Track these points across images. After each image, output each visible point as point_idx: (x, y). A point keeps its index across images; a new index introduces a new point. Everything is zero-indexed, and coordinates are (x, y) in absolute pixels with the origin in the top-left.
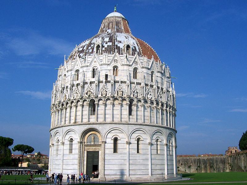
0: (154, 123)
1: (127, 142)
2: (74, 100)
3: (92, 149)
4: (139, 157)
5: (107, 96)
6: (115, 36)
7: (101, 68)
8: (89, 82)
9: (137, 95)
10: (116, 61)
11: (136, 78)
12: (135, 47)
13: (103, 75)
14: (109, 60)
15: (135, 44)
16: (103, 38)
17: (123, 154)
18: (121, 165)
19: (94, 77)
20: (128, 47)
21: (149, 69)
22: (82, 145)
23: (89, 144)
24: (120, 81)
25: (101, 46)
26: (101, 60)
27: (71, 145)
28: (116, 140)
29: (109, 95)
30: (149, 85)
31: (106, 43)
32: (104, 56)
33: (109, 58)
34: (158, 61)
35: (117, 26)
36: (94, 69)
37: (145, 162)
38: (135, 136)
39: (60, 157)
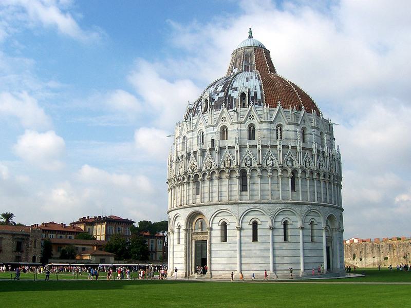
0: (278, 198)
3: (200, 238)
4: (255, 246)
8: (192, 152)
9: (251, 162)
10: (223, 119)
11: (254, 139)
12: (255, 93)
13: (208, 139)
14: (215, 119)
15: (258, 88)
17: (233, 243)
18: (231, 257)
20: (243, 95)
21: (271, 123)
22: (189, 234)
24: (227, 147)
25: (208, 99)
27: (179, 233)
30: (269, 145)
33: (215, 116)
34: (290, 107)
37: (265, 254)
38: (248, 218)
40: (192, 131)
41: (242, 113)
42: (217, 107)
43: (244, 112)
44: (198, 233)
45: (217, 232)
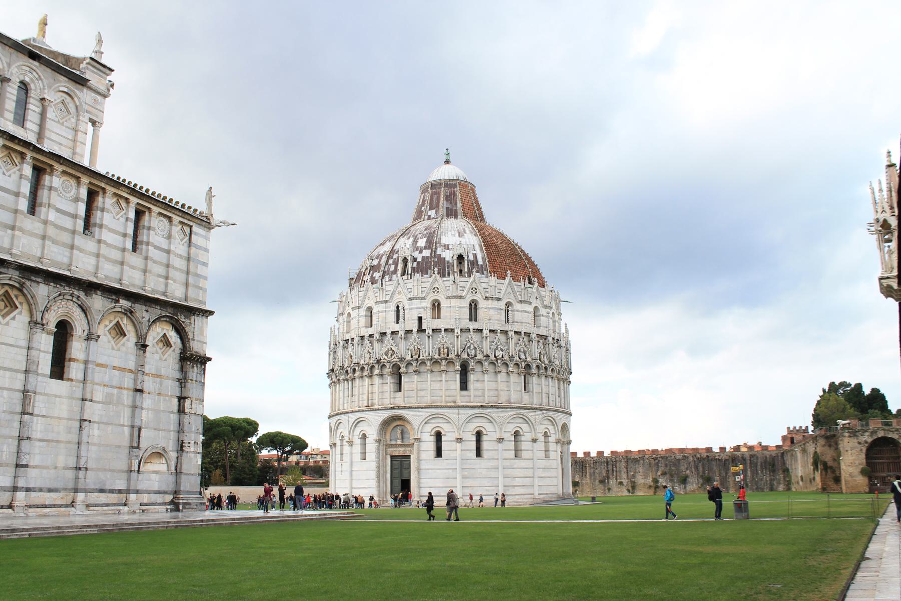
0: (509, 402)
3: (398, 452)
8: (389, 332)
10: (435, 290)
11: (476, 320)
12: (475, 256)
15: (477, 248)
20: (460, 258)
23: (393, 442)
25: (409, 258)
27: (364, 445)
28: (438, 436)
33: (423, 285)
35: (447, 200)
36: (398, 307)
39: (346, 466)
40: (386, 302)
41: (462, 284)
42: (423, 268)
43: (466, 283)
44: (396, 446)
45: (429, 445)
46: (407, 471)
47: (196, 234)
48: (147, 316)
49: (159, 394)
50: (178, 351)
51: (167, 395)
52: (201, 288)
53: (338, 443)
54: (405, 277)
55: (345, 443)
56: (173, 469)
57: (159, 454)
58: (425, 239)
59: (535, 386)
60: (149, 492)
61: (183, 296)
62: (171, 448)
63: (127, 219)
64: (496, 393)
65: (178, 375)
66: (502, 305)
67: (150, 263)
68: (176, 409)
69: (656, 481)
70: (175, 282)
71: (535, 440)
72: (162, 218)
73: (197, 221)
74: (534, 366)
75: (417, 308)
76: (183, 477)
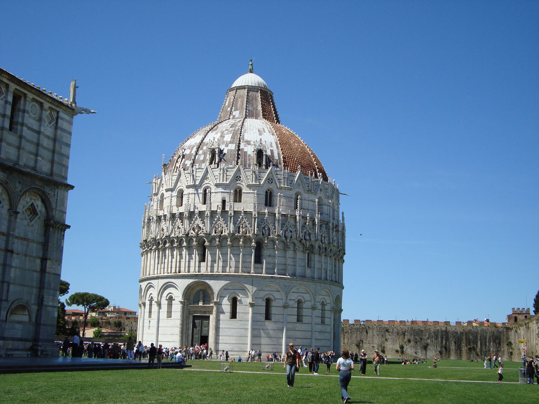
1: (250, 303)
2: (175, 238)
5: (223, 234)
6: (243, 130)
7: (215, 190)
12: (272, 151)
15: (274, 145)
16: (222, 136)
19: (205, 203)
20: (260, 153)
25: (217, 150)
26: (216, 177)
27: (170, 305)
29: (226, 234)
31: (227, 146)
32: (222, 172)
36: (205, 191)
39: (154, 322)
46: (206, 329)
47: (62, 119)
48: (19, 187)
49: (26, 255)
50: (43, 218)
51: (32, 256)
52: (64, 166)
53: (148, 303)
54: (213, 166)
55: (153, 302)
56: (34, 319)
57: (23, 307)
58: (231, 135)
59: (316, 263)
60: (13, 339)
61: (49, 172)
62: (33, 302)
63: (6, 102)
64: (284, 267)
65: (41, 239)
66: (293, 193)
67: (23, 141)
68: (38, 269)
69: (402, 347)
70: (43, 158)
71: (314, 308)
72: (35, 103)
73: (64, 108)
74: (317, 245)
75: (222, 192)
76: (42, 327)
